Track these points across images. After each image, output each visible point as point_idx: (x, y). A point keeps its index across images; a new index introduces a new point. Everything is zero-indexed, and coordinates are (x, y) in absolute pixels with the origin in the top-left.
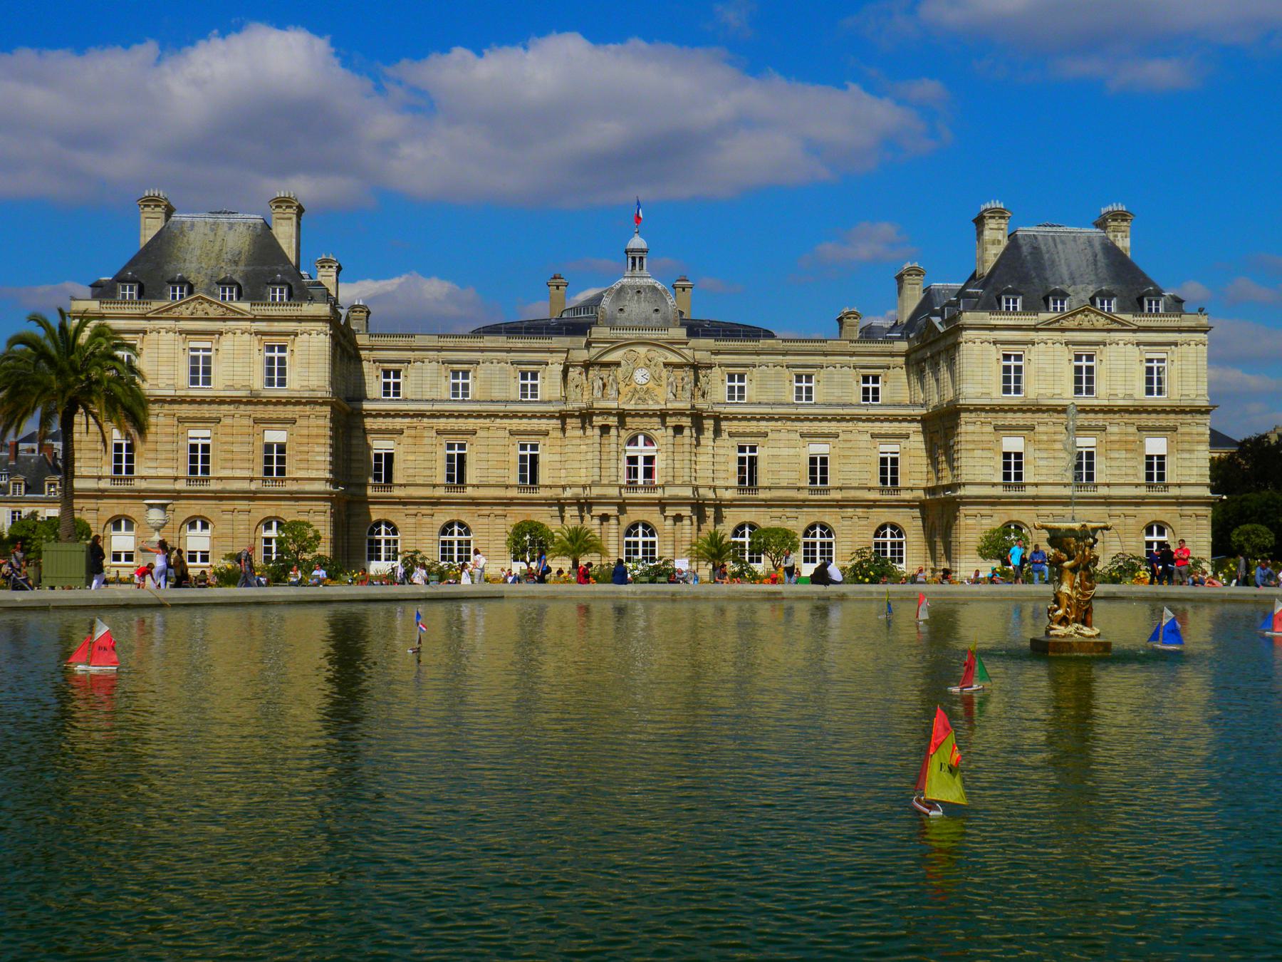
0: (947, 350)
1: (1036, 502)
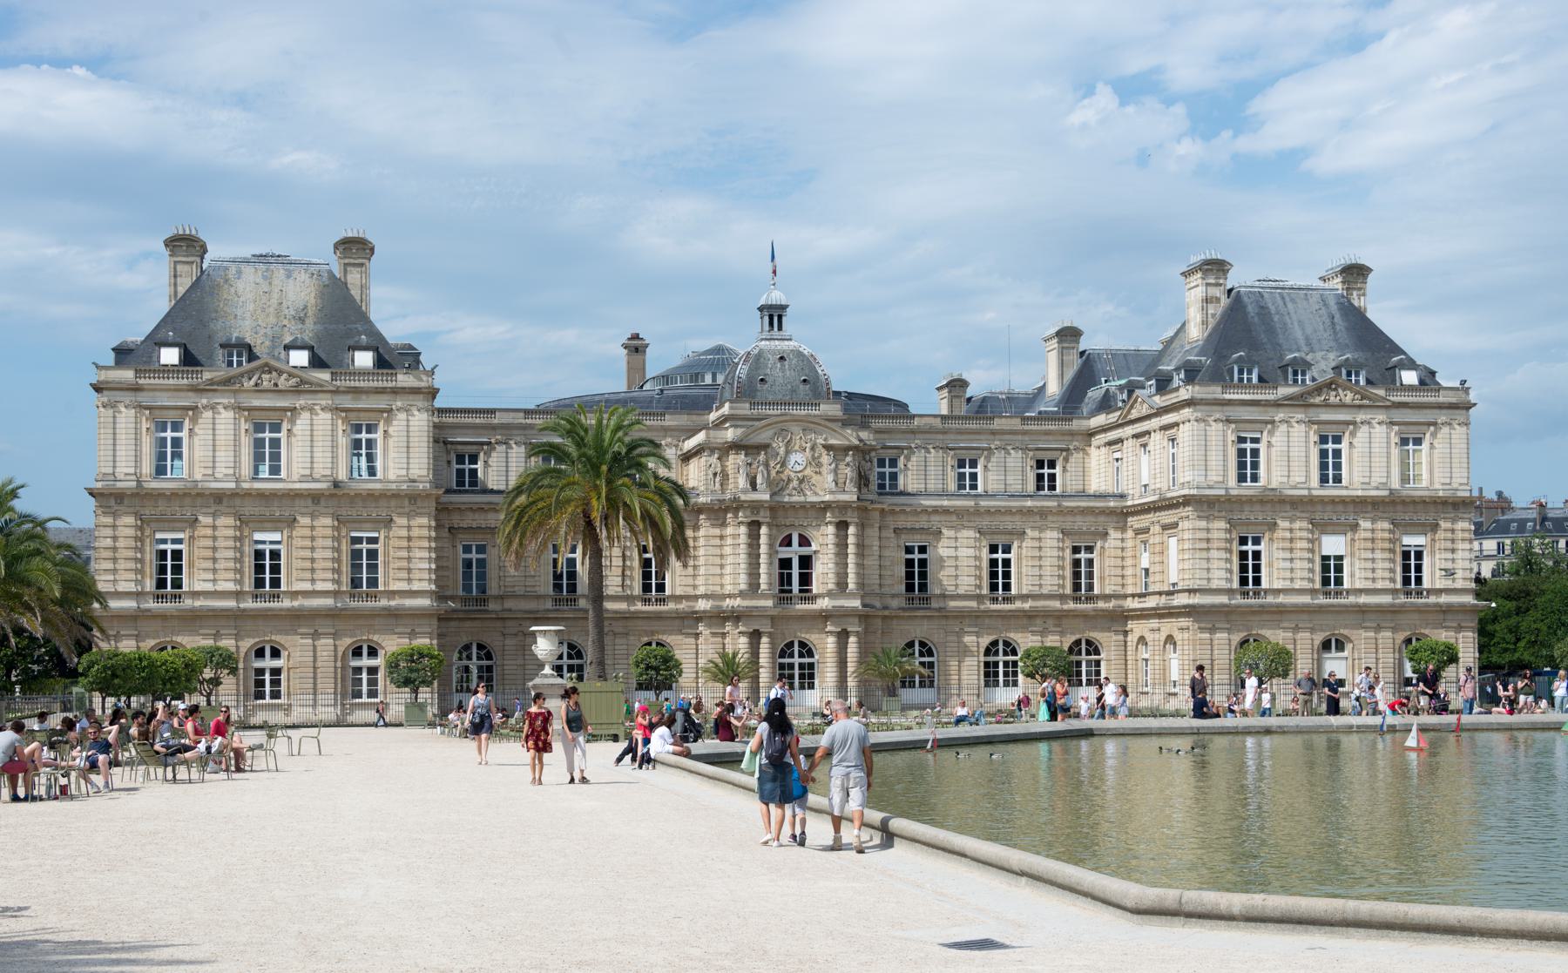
0: (1165, 428)
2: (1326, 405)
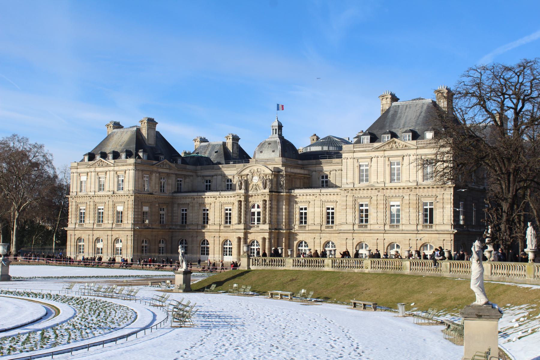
1: (371, 232)
2: (391, 149)
